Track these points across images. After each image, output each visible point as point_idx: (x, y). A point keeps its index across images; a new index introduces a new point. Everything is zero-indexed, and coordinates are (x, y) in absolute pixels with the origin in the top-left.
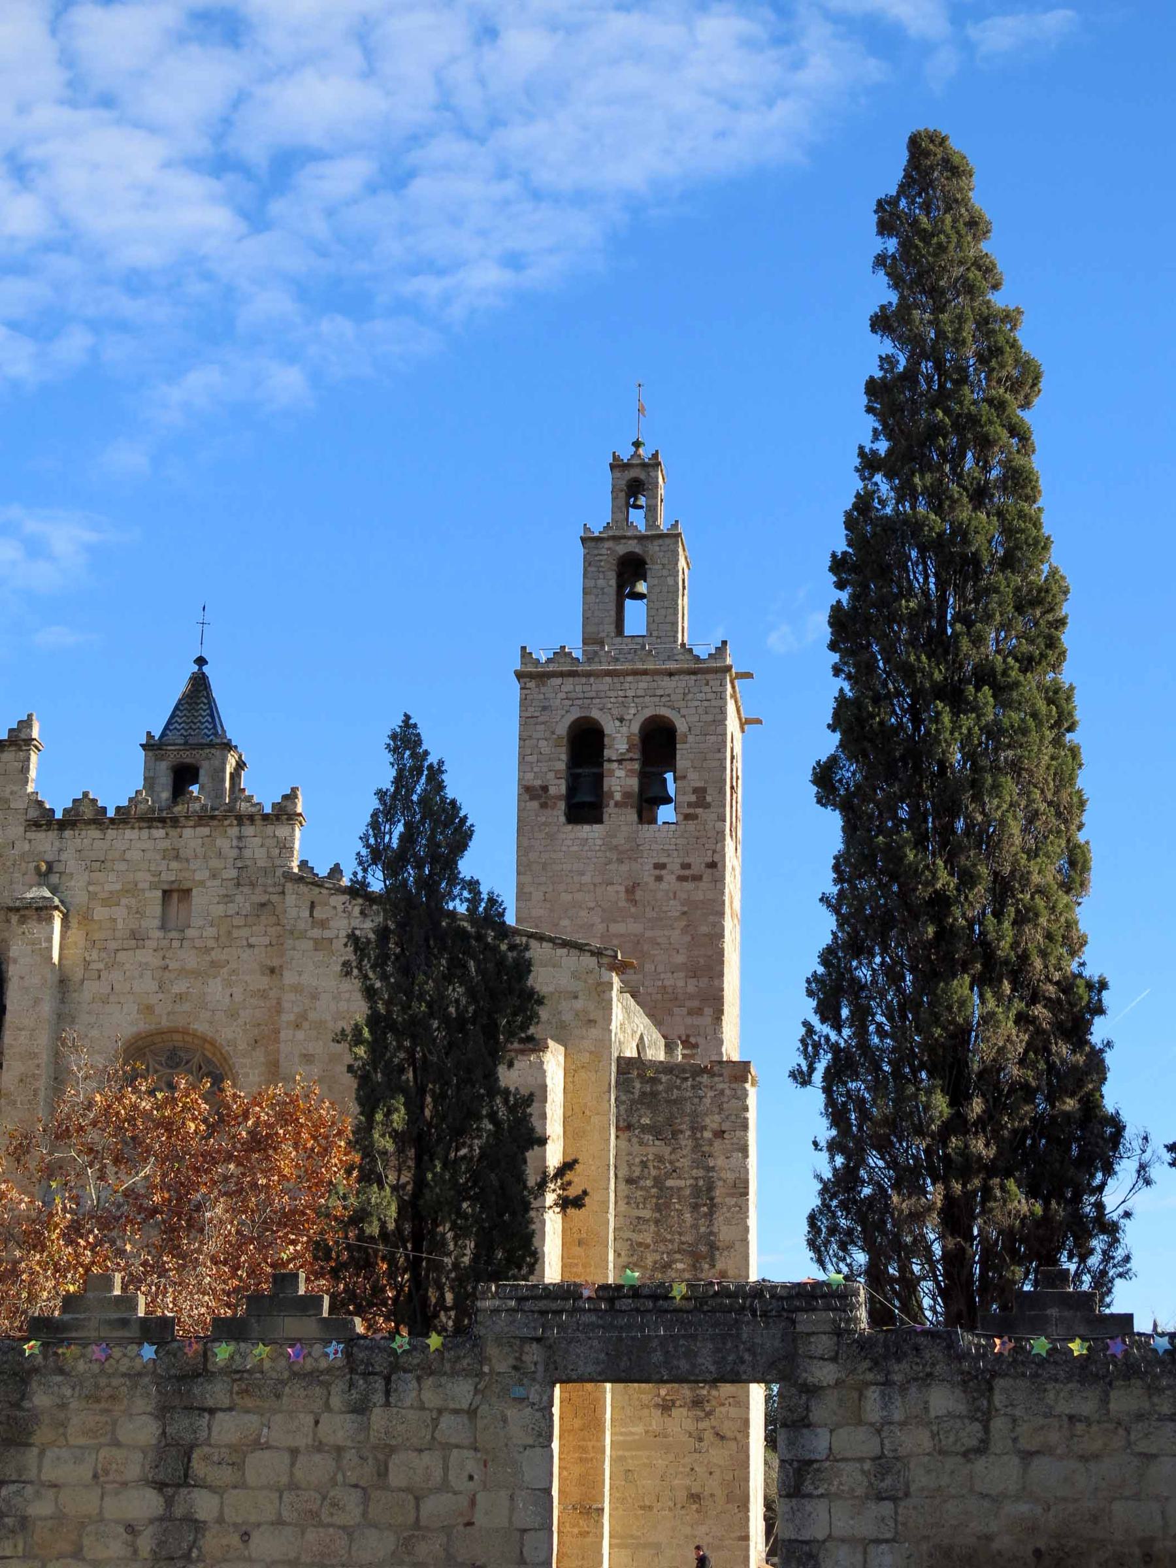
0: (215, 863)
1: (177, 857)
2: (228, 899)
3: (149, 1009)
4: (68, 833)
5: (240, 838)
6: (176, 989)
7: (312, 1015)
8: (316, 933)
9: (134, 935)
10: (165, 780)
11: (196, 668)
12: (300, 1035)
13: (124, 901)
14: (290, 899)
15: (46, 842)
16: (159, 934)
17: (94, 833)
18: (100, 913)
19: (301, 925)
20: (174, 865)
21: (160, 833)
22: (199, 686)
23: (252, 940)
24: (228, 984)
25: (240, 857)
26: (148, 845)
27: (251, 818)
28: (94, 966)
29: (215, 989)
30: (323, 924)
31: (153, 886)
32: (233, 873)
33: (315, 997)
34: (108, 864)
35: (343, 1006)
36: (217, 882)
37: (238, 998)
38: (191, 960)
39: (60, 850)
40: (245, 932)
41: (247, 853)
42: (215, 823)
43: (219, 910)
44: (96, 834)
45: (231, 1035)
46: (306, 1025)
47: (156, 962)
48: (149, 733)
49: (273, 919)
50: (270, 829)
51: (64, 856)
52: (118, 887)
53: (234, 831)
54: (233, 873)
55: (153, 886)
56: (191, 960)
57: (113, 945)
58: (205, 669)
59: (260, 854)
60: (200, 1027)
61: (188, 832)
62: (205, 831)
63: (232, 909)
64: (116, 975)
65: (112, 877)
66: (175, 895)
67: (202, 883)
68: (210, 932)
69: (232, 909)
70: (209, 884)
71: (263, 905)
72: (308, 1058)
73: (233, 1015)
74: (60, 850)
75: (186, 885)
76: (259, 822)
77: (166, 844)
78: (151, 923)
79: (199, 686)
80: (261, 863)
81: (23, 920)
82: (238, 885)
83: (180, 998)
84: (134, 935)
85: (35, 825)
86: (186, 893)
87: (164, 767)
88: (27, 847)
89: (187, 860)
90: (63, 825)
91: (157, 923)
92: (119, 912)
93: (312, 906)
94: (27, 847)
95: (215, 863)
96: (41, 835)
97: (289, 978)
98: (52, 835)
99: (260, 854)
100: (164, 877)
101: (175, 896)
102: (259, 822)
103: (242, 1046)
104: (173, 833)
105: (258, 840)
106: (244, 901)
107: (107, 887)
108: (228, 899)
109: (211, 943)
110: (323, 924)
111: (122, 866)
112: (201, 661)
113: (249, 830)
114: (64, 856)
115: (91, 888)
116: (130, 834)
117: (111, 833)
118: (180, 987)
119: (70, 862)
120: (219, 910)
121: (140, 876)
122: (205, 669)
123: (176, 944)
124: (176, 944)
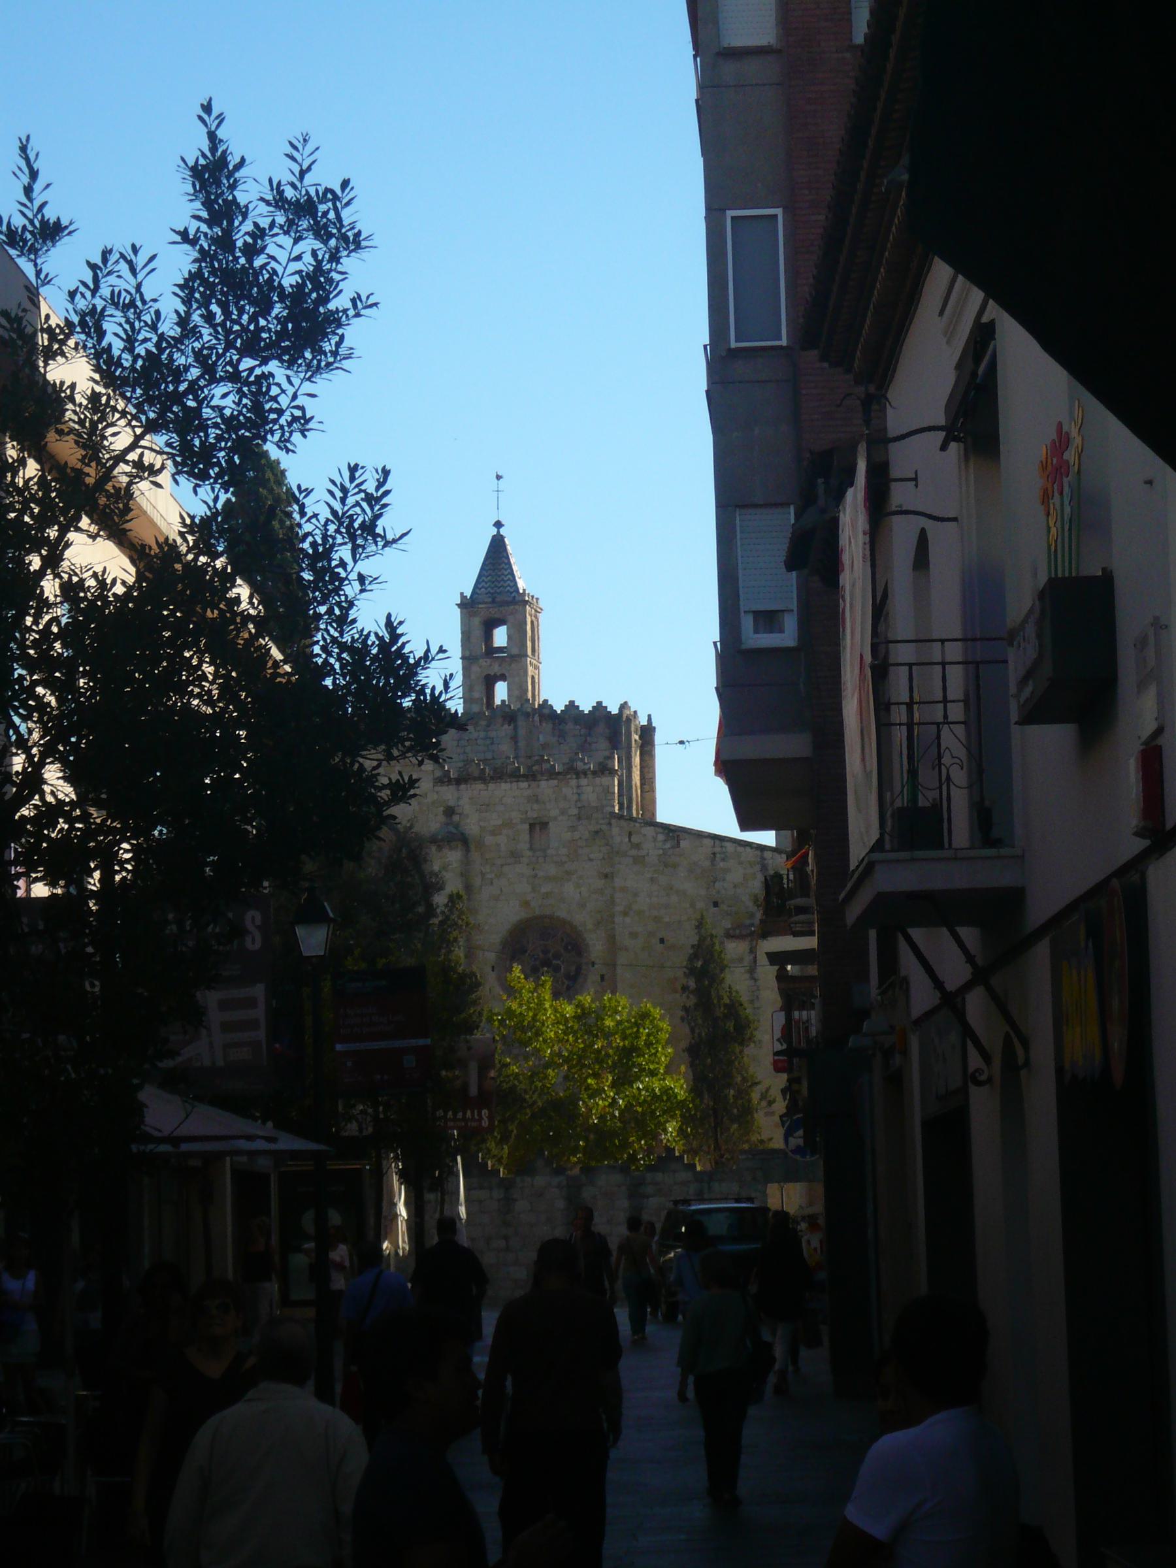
1: (537, 801)
2: (573, 828)
3: (527, 904)
4: (463, 786)
5: (578, 787)
6: (543, 890)
8: (634, 852)
10: (478, 632)
11: (494, 531)
12: (628, 920)
13: (505, 832)
14: (615, 830)
16: (529, 853)
17: (480, 786)
18: (489, 840)
20: (535, 806)
21: (525, 784)
22: (497, 552)
23: (592, 856)
25: (579, 800)
27: (585, 773)
28: (489, 876)
29: (569, 889)
30: (638, 846)
31: (523, 821)
32: (575, 811)
33: (636, 895)
39: (459, 799)
41: (584, 797)
42: (560, 777)
43: (568, 836)
45: (582, 919)
48: (462, 594)
50: (598, 780)
52: (500, 822)
53: (573, 782)
55: (523, 821)
56: (552, 870)
58: (503, 531)
60: (562, 914)
61: (543, 784)
62: (556, 782)
63: (577, 835)
66: (538, 826)
67: (555, 818)
68: (564, 851)
69: (577, 835)
70: (560, 818)
71: (597, 832)
72: (634, 935)
73: (582, 906)
74: (459, 799)
75: (546, 820)
76: (590, 776)
77: (529, 792)
78: (523, 846)
79: (497, 552)
80: (594, 804)
81: (440, 848)
82: (579, 819)
83: (547, 895)
86: (544, 825)
87: (477, 621)
89: (544, 803)
90: (459, 781)
91: (528, 845)
93: (630, 834)
94: (435, 797)
96: (445, 788)
97: (618, 882)
98: (452, 788)
100: (530, 814)
101: (538, 828)
102: (590, 776)
103: (590, 926)
104: (534, 784)
105: (590, 789)
108: (573, 828)
110: (638, 846)
112: (498, 525)
113: (583, 781)
115: (482, 824)
116: (505, 786)
117: (491, 786)
119: (466, 806)
120: (568, 836)
122: (503, 531)
123: (541, 860)
124: (541, 860)
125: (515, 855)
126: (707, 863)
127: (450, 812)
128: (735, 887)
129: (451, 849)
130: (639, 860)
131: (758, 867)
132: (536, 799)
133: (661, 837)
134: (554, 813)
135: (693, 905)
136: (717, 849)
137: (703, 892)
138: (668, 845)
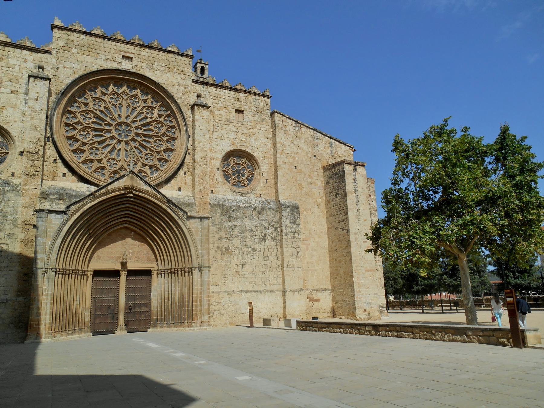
0: (249, 105)
2: (254, 115)
4: (205, 86)
6: (241, 139)
7: (285, 151)
8: (284, 129)
9: (228, 121)
12: (282, 156)
13: (224, 110)
15: (200, 88)
18: (217, 112)
19: (280, 126)
20: (238, 102)
21: (233, 93)
24: (256, 139)
26: (230, 95)
29: (252, 141)
32: (255, 109)
33: (285, 146)
34: (218, 98)
35: (292, 150)
36: (251, 110)
37: (259, 144)
38: (245, 131)
40: (259, 126)
41: (258, 104)
43: (252, 118)
44: (215, 89)
46: (284, 154)
47: (235, 129)
49: (266, 124)
50: (263, 99)
51: (205, 93)
53: (254, 97)
54: (255, 109)
57: (222, 122)
59: (262, 105)
64: (224, 131)
65: (220, 102)
73: (258, 148)
75: (242, 109)
84: (228, 121)
85: (194, 81)
88: (193, 88)
92: (223, 113)
95: (249, 105)
98: (201, 86)
99: (262, 105)
104: (237, 94)
106: (258, 117)
107: (219, 105)
109: (250, 127)
111: (223, 100)
113: (258, 97)
114: (205, 93)
118: (242, 137)
120: (252, 118)
121: (228, 104)
123: (240, 125)
125: (229, 121)
126: (312, 139)
127: (199, 96)
128: (322, 150)
129: (204, 110)
130: (285, 132)
131: (329, 145)
132: (238, 100)
133: (294, 125)
134: (246, 107)
135: (307, 154)
136: (315, 135)
137: (311, 150)
138: (297, 129)
